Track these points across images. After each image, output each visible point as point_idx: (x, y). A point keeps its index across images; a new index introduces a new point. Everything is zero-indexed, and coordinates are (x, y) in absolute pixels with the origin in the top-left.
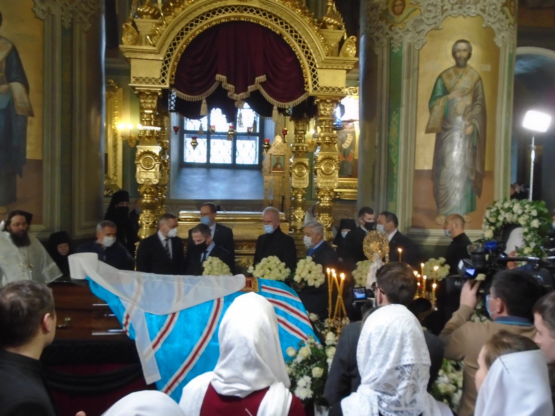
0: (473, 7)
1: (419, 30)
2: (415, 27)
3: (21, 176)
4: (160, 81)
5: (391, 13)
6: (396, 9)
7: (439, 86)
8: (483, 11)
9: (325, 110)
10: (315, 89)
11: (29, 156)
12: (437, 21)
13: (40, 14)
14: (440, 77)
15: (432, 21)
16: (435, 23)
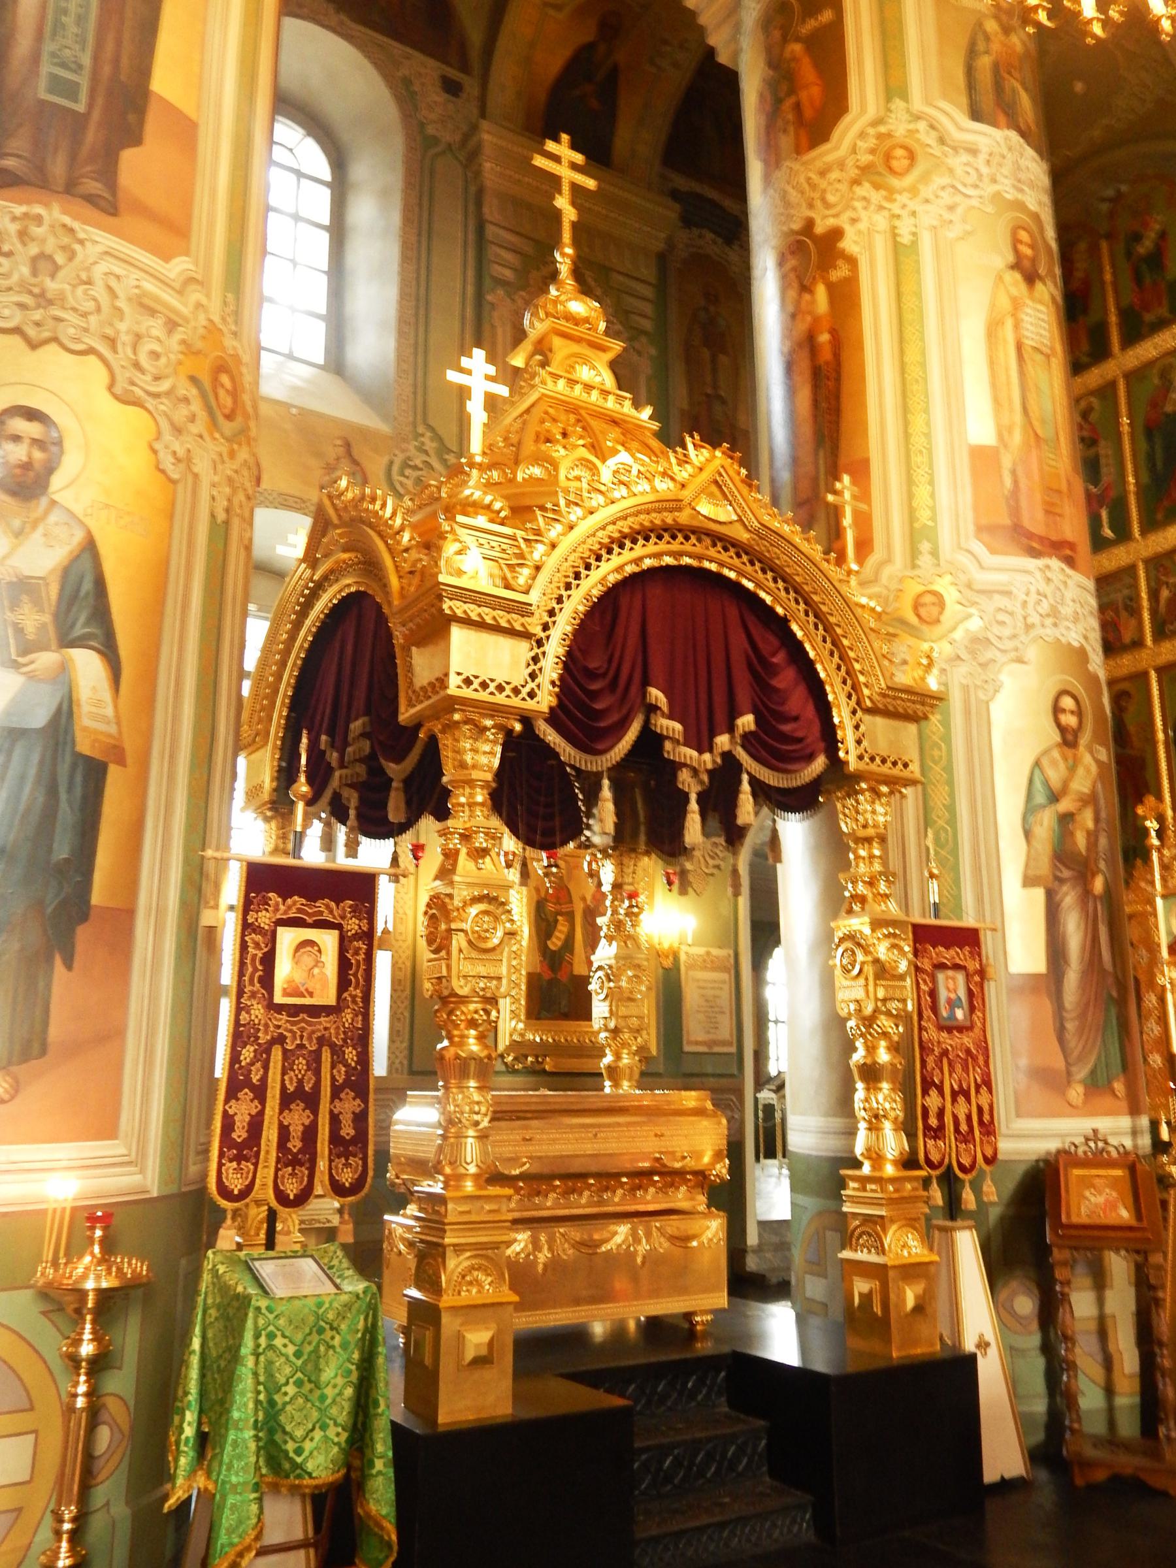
0: (1071, 625)
1: (982, 660)
2: (973, 653)
3: (69, 966)
4: (525, 691)
5: (913, 620)
6: (923, 612)
7: (1038, 785)
8: (1086, 638)
9: (874, 812)
10: (861, 757)
11: (97, 897)
12: (1020, 646)
13: (167, 462)
14: (1037, 764)
15: (1009, 645)
16: (1016, 649)
